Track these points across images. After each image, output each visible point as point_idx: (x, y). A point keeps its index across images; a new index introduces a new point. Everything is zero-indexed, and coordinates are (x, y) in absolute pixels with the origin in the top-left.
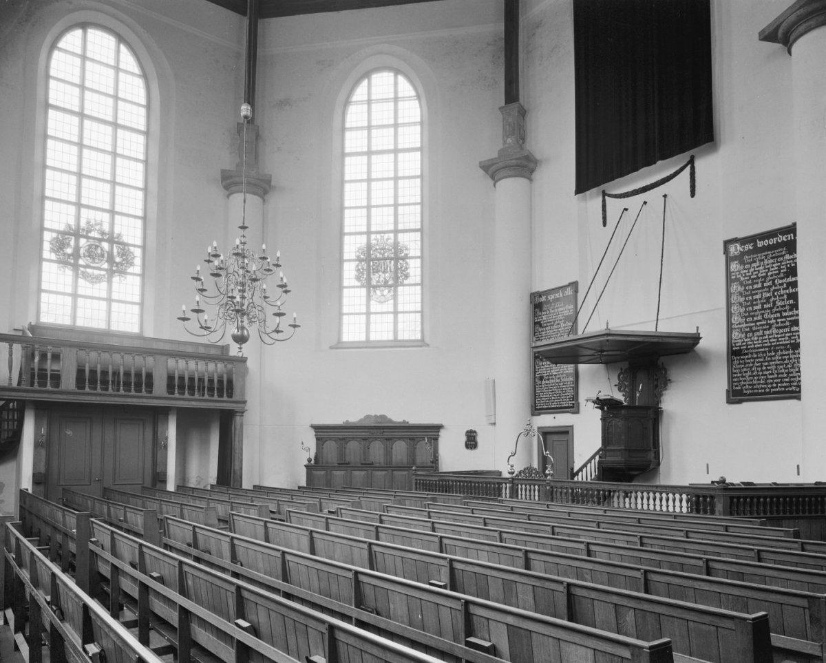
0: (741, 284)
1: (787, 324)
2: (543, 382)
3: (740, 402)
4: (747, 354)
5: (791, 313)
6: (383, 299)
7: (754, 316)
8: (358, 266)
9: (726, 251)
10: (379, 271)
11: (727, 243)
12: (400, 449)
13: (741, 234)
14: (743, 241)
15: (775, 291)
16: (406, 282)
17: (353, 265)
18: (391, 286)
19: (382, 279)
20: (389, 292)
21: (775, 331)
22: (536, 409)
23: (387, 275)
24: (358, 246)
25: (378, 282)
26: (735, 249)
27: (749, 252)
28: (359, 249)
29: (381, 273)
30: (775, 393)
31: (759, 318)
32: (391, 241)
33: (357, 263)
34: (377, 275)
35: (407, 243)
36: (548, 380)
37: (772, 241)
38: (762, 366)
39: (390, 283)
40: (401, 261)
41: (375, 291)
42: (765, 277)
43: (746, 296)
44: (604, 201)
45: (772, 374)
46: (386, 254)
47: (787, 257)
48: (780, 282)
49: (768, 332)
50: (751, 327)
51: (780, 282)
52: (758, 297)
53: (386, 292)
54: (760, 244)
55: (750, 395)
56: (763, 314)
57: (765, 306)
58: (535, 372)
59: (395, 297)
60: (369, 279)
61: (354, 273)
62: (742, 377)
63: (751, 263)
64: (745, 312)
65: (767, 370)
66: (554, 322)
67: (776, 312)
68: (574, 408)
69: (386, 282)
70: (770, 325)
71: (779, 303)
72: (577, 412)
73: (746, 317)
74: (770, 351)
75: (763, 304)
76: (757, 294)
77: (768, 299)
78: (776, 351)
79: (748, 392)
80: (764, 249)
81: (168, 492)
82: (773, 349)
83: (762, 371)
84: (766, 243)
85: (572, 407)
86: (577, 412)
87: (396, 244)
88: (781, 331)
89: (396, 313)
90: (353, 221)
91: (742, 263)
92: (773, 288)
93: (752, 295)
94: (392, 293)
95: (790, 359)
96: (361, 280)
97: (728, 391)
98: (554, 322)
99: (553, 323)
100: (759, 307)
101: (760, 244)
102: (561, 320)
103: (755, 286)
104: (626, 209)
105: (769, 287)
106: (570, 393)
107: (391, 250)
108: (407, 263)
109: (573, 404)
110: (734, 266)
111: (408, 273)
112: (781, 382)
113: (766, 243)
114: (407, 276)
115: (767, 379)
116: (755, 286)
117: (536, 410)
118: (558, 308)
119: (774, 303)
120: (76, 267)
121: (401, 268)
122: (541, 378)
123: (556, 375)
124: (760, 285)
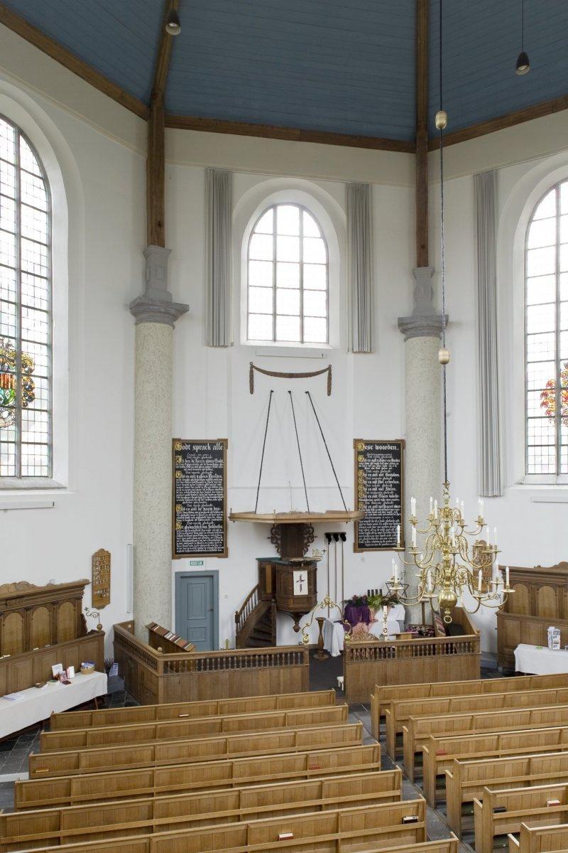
0: (365, 471)
1: (392, 503)
2: (186, 527)
3: (362, 551)
4: (368, 520)
5: (394, 497)
7: (372, 495)
9: (355, 447)
11: (356, 441)
13: (366, 438)
14: (368, 443)
15: (385, 480)
16: (30, 405)
18: (12, 407)
20: (10, 414)
21: (385, 507)
22: (176, 553)
26: (362, 447)
27: (370, 451)
30: (384, 547)
31: (376, 496)
32: (13, 348)
35: (31, 356)
36: (193, 525)
37: (384, 448)
38: (376, 528)
39: (11, 403)
40: (25, 378)
42: (380, 470)
43: (368, 480)
44: (251, 372)
45: (383, 534)
46: (6, 364)
47: (393, 460)
48: (389, 475)
49: (380, 507)
50: (371, 502)
51: (389, 475)
52: (375, 482)
54: (377, 448)
55: (369, 547)
56: (378, 495)
57: (380, 489)
58: (176, 517)
59: (18, 422)
62: (365, 535)
63: (371, 459)
64: (367, 491)
65: (380, 531)
66: (201, 472)
67: (386, 494)
68: (222, 552)
70: (382, 502)
71: (387, 489)
72: (226, 556)
73: (368, 495)
74: (382, 519)
75: (378, 488)
76: (374, 480)
77: (381, 485)
78: (385, 519)
79: (368, 545)
80: (379, 451)
82: (384, 518)
83: (377, 532)
84: (381, 448)
85: (222, 552)
86: (226, 556)
87: (19, 353)
88: (388, 507)
89: (19, 443)
91: (366, 457)
92: (384, 478)
93: (372, 480)
94: (13, 416)
95: (393, 525)
97: (355, 544)
98: (201, 472)
99: (199, 473)
100: (376, 489)
101: (377, 448)
102: (209, 471)
103: (374, 475)
104: (272, 391)
105: (382, 477)
106: (218, 539)
108: (32, 382)
109: (223, 549)
110: (361, 458)
111: (33, 395)
112: (388, 540)
113: (381, 448)
114: (31, 398)
115: (379, 537)
116: (374, 475)
117: (177, 553)
118: (205, 459)
119: (385, 488)
121: (25, 385)
122: (184, 524)
123: (202, 522)
124: (376, 475)
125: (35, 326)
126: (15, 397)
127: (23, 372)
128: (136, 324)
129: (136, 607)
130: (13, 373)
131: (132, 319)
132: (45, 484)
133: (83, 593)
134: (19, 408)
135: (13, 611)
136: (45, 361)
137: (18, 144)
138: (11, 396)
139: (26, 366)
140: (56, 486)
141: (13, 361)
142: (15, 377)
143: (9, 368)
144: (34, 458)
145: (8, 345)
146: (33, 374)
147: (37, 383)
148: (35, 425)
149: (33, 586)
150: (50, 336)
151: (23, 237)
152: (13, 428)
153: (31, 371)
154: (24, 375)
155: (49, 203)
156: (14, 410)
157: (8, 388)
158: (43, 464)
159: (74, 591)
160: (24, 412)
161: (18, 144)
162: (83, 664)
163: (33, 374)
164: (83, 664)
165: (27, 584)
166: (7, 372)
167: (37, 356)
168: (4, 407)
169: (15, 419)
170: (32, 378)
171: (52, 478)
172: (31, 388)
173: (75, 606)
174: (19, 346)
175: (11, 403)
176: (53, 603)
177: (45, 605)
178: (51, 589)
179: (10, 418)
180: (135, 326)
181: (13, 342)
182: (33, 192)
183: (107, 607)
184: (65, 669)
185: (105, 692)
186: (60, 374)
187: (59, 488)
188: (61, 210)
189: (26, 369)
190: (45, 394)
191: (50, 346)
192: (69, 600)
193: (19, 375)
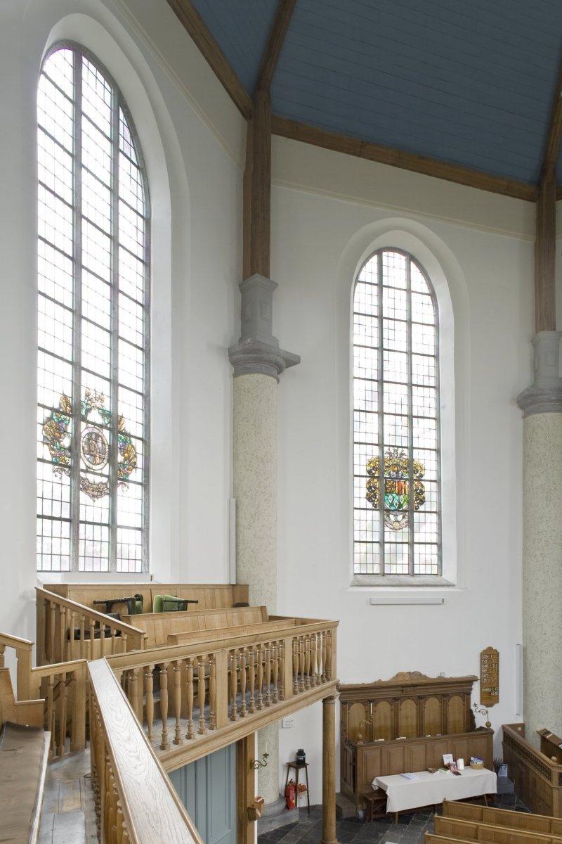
6: (396, 525)
8: (369, 482)
10: (393, 492)
12: (432, 707)
16: (422, 508)
17: (364, 481)
18: (405, 511)
19: (396, 502)
20: (404, 517)
23: (402, 496)
24: (369, 458)
25: (392, 505)
28: (370, 462)
29: (394, 495)
33: (368, 479)
34: (391, 497)
35: (422, 462)
39: (405, 507)
40: (416, 483)
41: (388, 516)
46: (400, 472)
53: (400, 517)
59: (411, 524)
60: (382, 501)
61: (364, 492)
69: (400, 506)
81: (323, 803)
89: (411, 544)
90: (365, 429)
96: (373, 501)
107: (406, 468)
108: (422, 486)
111: (424, 498)
114: (422, 502)
120: (73, 471)
121: (416, 490)
125: (425, 434)
126: (408, 502)
127: (415, 478)
128: (524, 417)
129: (526, 710)
130: (407, 479)
131: (520, 413)
132: (436, 582)
133: (471, 689)
134: (411, 511)
135: (409, 698)
136: (434, 465)
137: (409, 270)
138: (405, 501)
139: (417, 472)
140: (445, 583)
141: (406, 468)
142: (407, 483)
143: (402, 475)
144: (426, 557)
145: (402, 454)
146: (423, 478)
147: (427, 486)
148: (426, 527)
149: (425, 677)
150: (439, 441)
151: (414, 353)
152: (406, 529)
153: (422, 476)
154: (416, 480)
155: (437, 316)
156: (407, 514)
157: (402, 494)
158: (427, 563)
159: (463, 685)
160: (416, 515)
161: (409, 270)
162: (472, 759)
163: (423, 478)
164: (472, 759)
165: (420, 675)
166: (402, 479)
167: (426, 460)
168: (399, 511)
169: (408, 522)
170: (423, 482)
171: (441, 575)
172: (422, 492)
173: (464, 701)
174: (411, 454)
175: (405, 507)
176: (444, 695)
177: (435, 696)
178: (442, 681)
179: (404, 521)
180: (522, 420)
181: (406, 451)
182: (423, 310)
183: (496, 706)
184: (455, 760)
185: (495, 791)
186: (448, 476)
187: (448, 586)
188: (448, 321)
189: (418, 475)
190: (434, 497)
191: (438, 451)
192: (458, 694)
193: (411, 480)
